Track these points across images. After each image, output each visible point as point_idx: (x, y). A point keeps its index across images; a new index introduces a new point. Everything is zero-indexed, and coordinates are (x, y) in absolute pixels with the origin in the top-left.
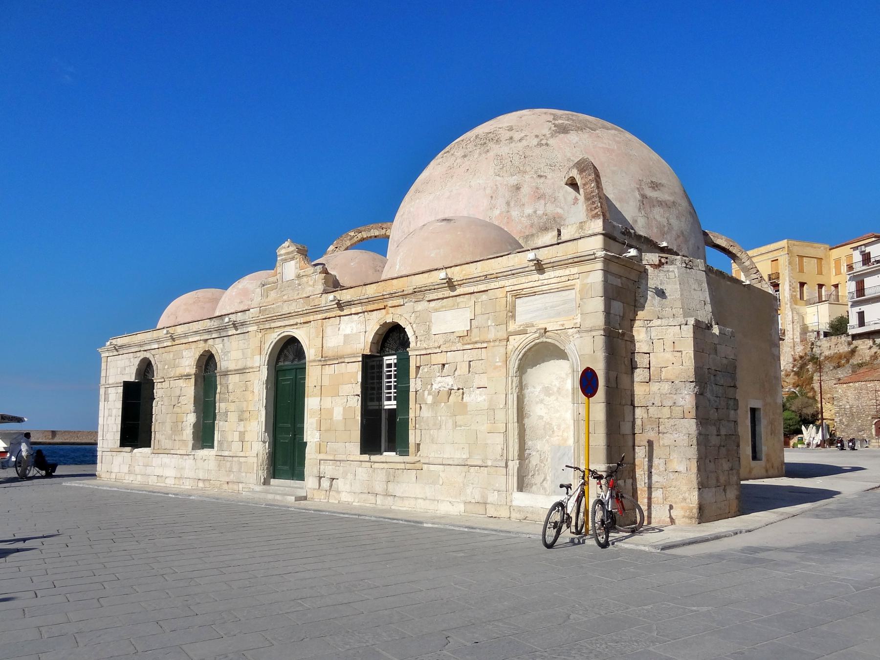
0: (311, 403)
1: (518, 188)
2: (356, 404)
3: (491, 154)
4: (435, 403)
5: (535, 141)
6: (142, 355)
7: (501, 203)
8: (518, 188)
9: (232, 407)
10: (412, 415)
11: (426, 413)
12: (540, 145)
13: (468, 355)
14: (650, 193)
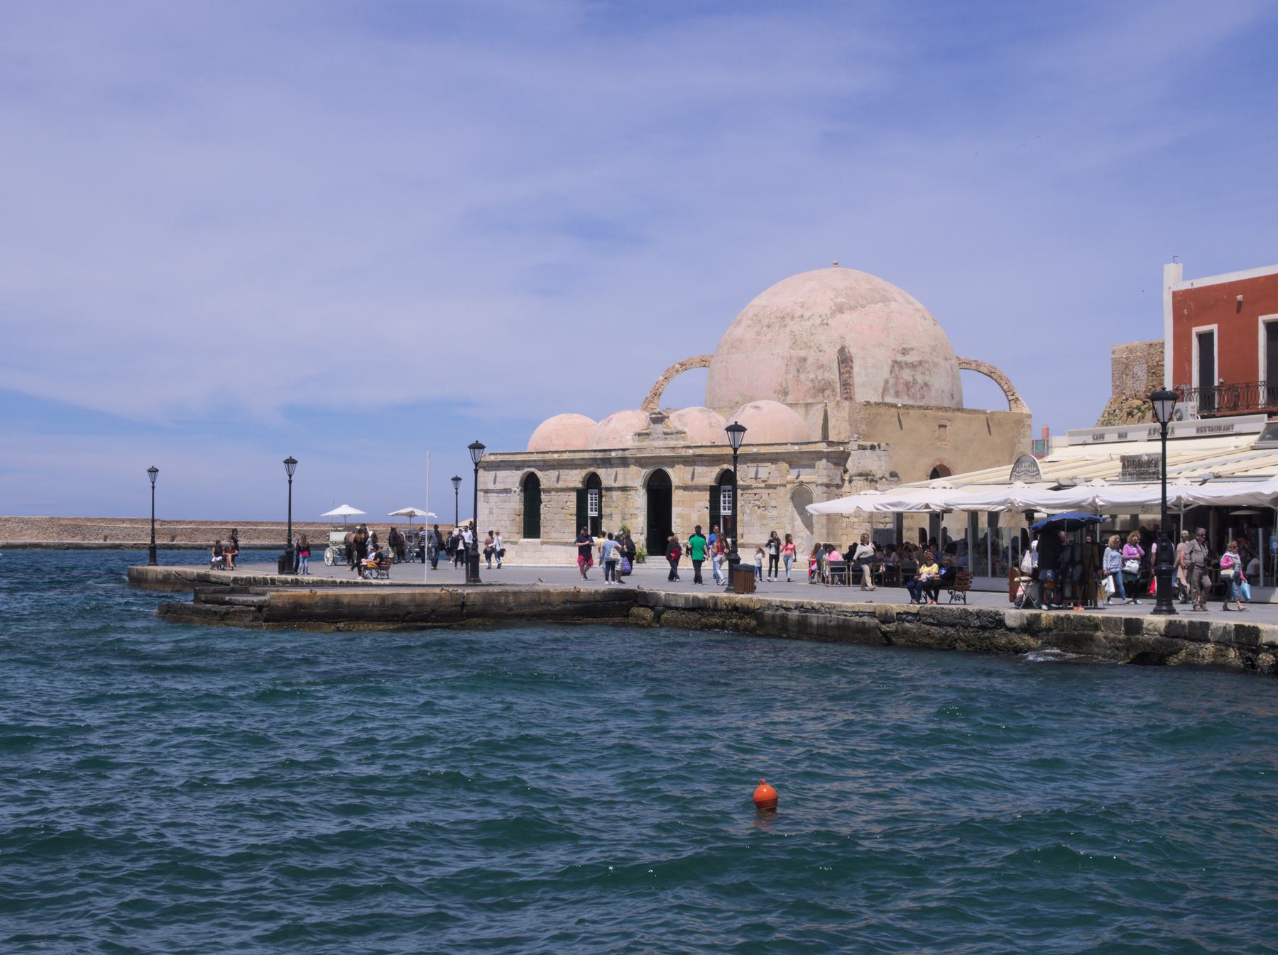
0: (675, 510)
1: (805, 360)
2: (707, 511)
3: (787, 329)
4: (751, 514)
5: (818, 321)
6: (526, 470)
7: (793, 369)
8: (805, 360)
9: (617, 511)
10: (739, 518)
11: (746, 518)
12: (822, 324)
13: (768, 491)
14: (900, 358)
